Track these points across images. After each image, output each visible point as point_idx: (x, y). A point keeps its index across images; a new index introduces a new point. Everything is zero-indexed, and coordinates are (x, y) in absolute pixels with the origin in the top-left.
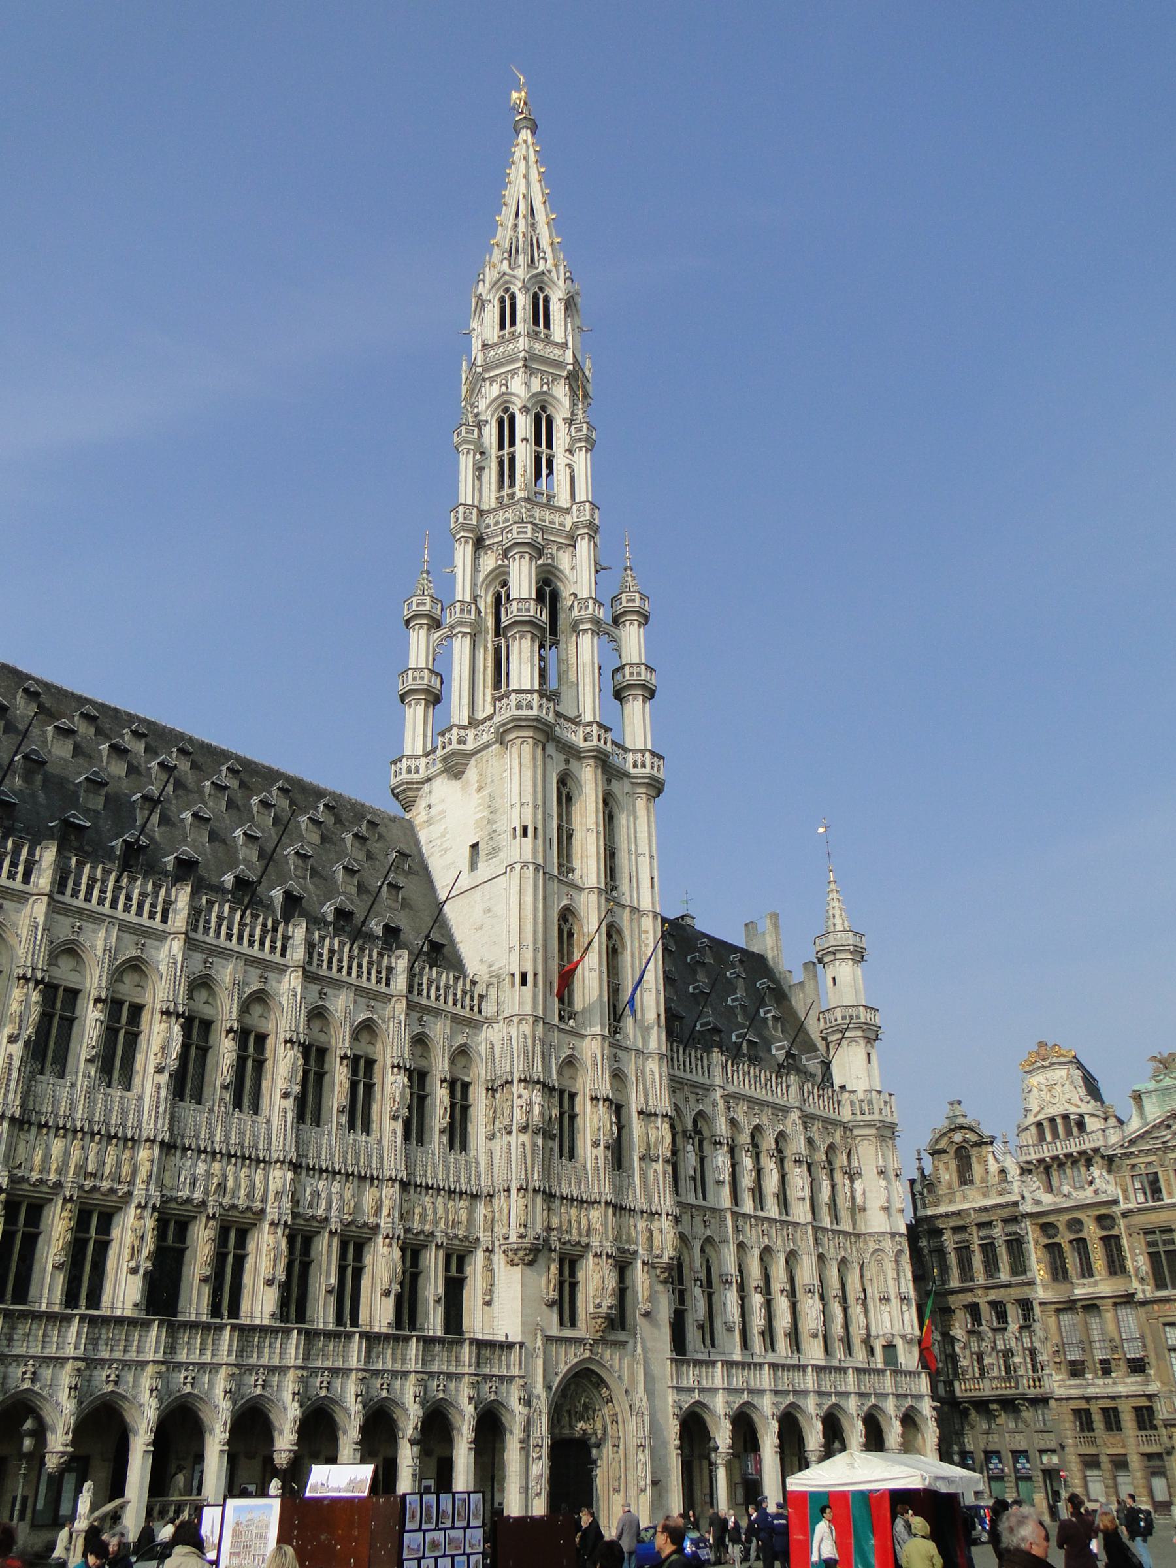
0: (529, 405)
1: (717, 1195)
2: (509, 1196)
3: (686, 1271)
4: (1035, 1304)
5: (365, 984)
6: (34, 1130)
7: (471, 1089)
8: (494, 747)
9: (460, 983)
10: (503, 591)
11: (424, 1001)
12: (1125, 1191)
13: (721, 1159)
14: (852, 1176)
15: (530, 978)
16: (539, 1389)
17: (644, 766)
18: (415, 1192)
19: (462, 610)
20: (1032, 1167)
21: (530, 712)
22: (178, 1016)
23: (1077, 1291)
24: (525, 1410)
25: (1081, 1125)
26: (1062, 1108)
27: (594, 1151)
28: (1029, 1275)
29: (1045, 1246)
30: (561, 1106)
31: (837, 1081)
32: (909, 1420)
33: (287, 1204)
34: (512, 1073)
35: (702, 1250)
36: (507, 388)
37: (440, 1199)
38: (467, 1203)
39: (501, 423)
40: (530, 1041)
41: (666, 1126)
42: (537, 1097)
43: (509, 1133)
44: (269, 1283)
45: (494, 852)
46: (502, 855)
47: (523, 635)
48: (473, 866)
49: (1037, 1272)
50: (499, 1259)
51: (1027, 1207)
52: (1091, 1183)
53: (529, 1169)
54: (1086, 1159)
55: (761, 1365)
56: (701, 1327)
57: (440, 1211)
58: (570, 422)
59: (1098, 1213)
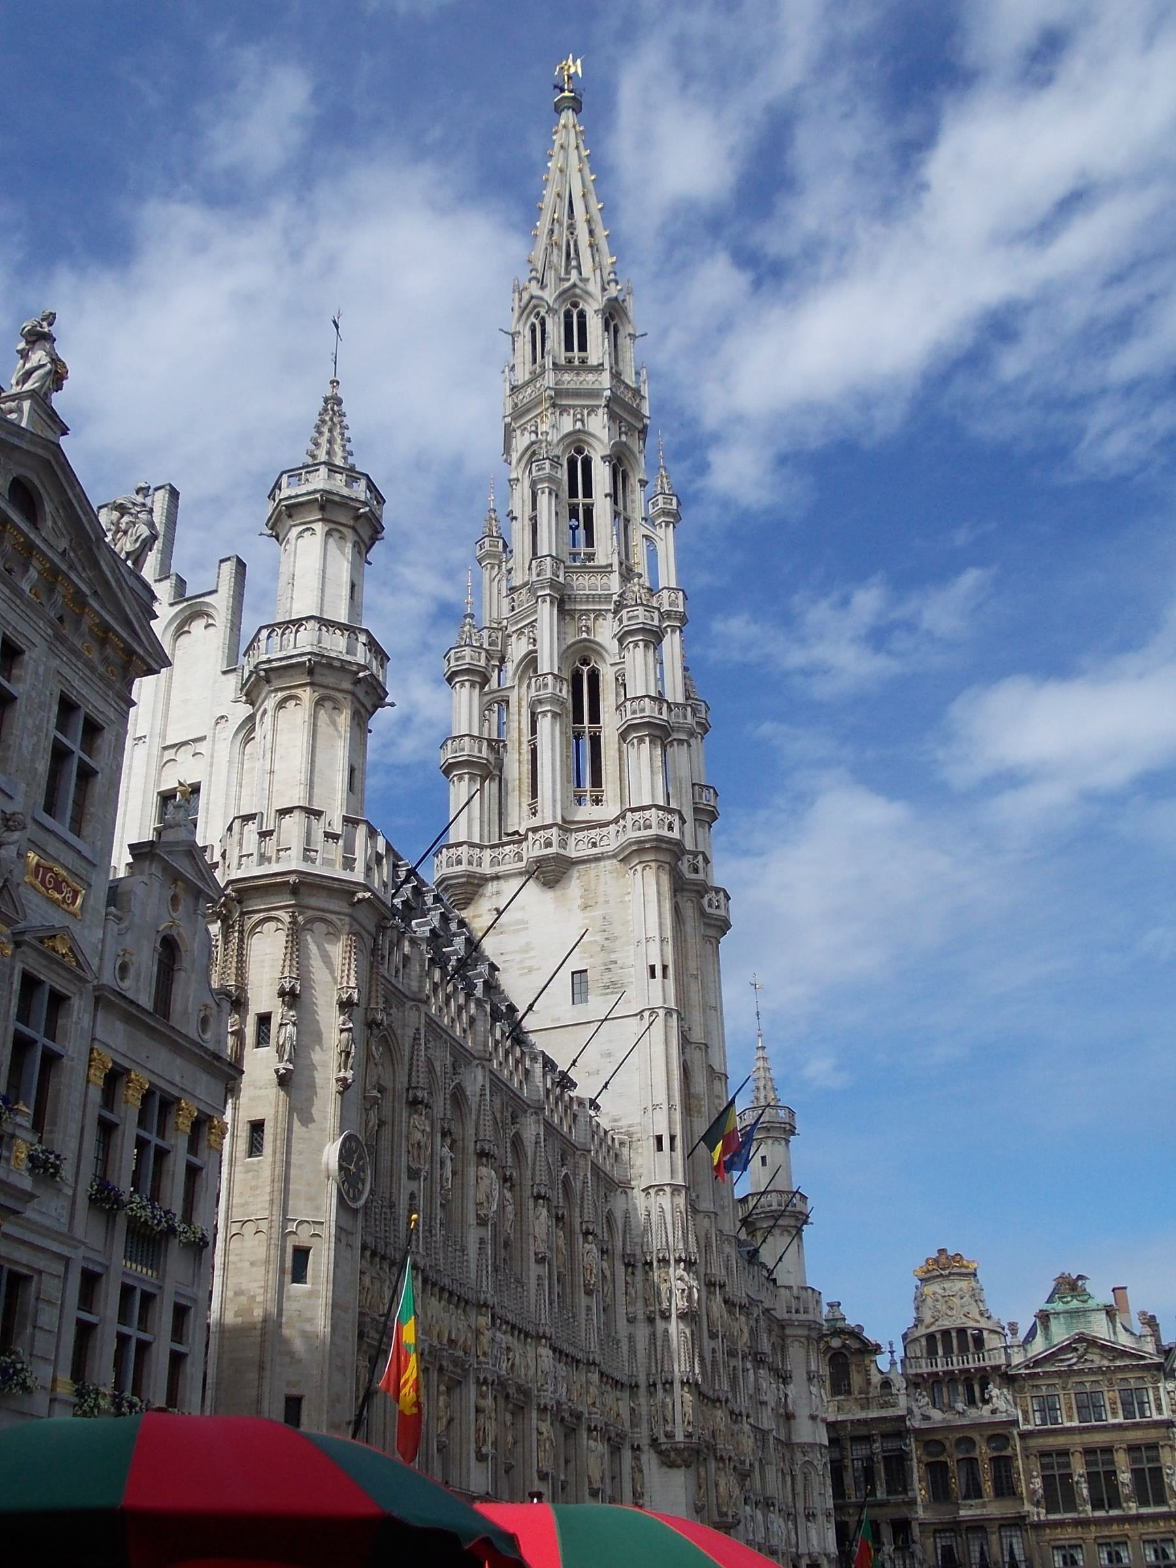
4: (915, 1525)
8: (608, 862)
10: (585, 669)
12: (1025, 1413)
20: (920, 1380)
21: (670, 834)
23: (962, 1513)
26: (959, 1321)
28: (910, 1493)
29: (928, 1465)
36: (584, 425)
39: (572, 463)
43: (666, 1317)
49: (918, 1492)
50: (649, 1459)
51: (917, 1424)
54: (984, 1377)
59: (990, 1433)
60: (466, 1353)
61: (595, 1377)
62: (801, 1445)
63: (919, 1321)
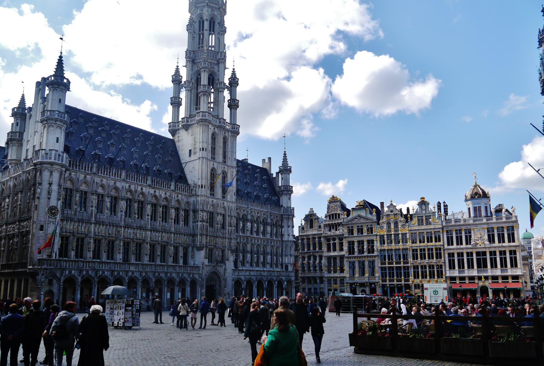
0: (208, 19)
1: (247, 233)
2: (197, 236)
3: (238, 250)
6: (98, 225)
11: (178, 192)
13: (249, 224)
14: (282, 227)
17: (234, 128)
19: (188, 83)
25: (339, 217)
30: (210, 215)
31: (281, 204)
32: (289, 282)
33: (149, 239)
35: (243, 245)
41: (235, 219)
42: (205, 214)
44: (146, 255)
45: (195, 153)
46: (198, 154)
47: (204, 95)
48: (190, 155)
52: (339, 230)
54: (339, 224)
55: (254, 270)
56: (241, 262)
58: (219, 23)
61: (173, 235)
62: (285, 241)
63: (328, 212)
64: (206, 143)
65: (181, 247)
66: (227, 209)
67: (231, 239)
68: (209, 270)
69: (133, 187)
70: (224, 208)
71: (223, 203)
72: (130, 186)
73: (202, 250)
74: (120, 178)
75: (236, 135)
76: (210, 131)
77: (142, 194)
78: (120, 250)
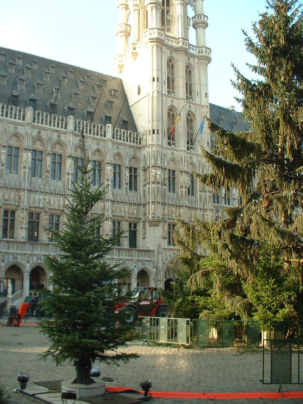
5: (96, 136)
7: (138, 170)
9: (132, 134)
11: (119, 141)
15: (156, 132)
16: (160, 264)
18: (117, 204)
22: (30, 150)
24: (154, 270)
27: (182, 190)
34: (150, 164)
37: (126, 206)
38: (137, 207)
40: (156, 153)
43: (149, 184)
48: (139, 93)
50: (147, 225)
53: (156, 196)
57: (126, 209)
60: (15, 202)
61: (109, 204)
64: (158, 70)
65: (124, 222)
66: (198, 165)
67: (205, 210)
68: (170, 257)
69: (44, 134)
70: (192, 164)
71: (191, 157)
72: (39, 133)
73: (157, 226)
74: (24, 120)
75: (205, 62)
76: (163, 56)
77: (59, 143)
78: (21, 223)
